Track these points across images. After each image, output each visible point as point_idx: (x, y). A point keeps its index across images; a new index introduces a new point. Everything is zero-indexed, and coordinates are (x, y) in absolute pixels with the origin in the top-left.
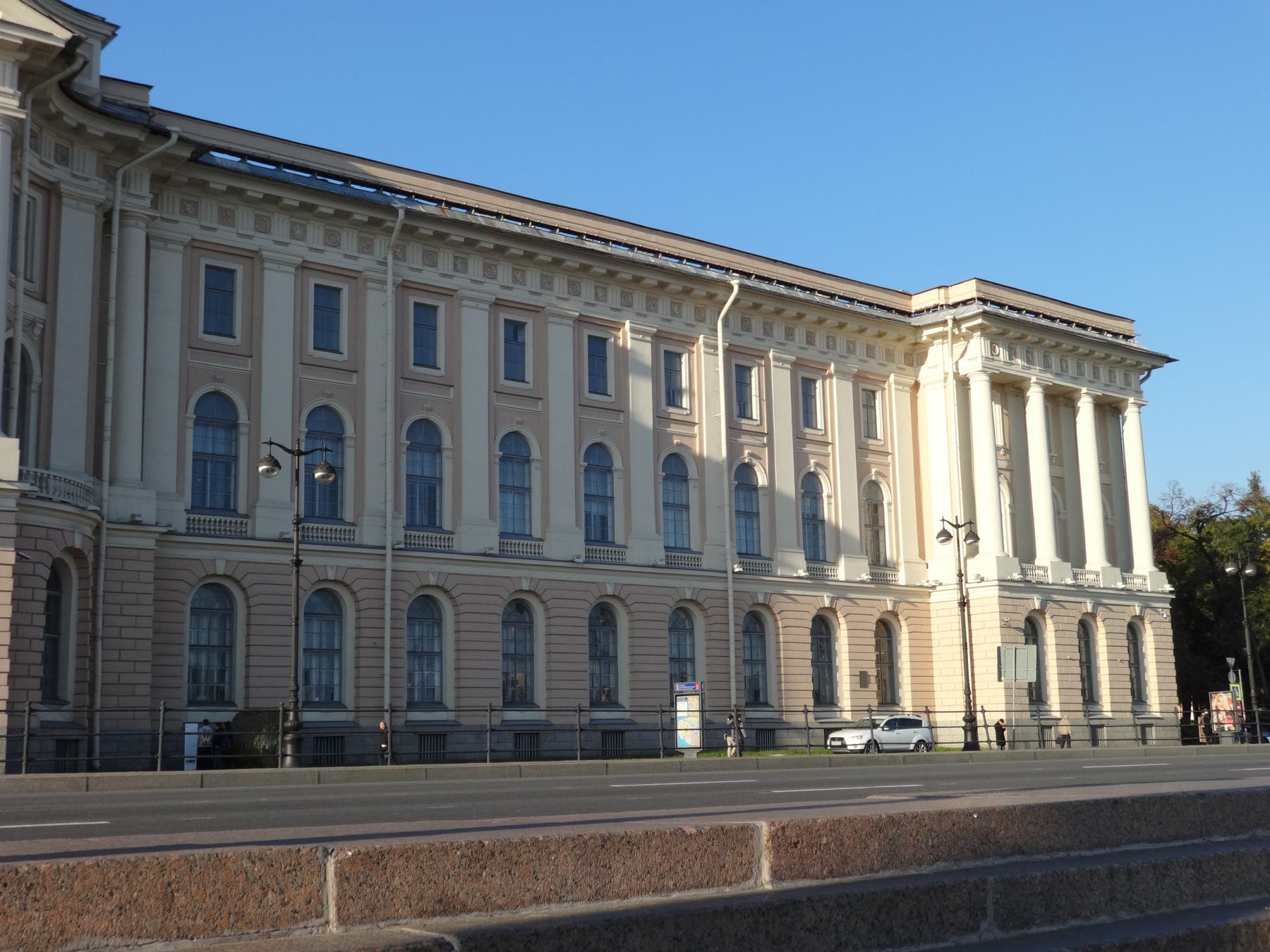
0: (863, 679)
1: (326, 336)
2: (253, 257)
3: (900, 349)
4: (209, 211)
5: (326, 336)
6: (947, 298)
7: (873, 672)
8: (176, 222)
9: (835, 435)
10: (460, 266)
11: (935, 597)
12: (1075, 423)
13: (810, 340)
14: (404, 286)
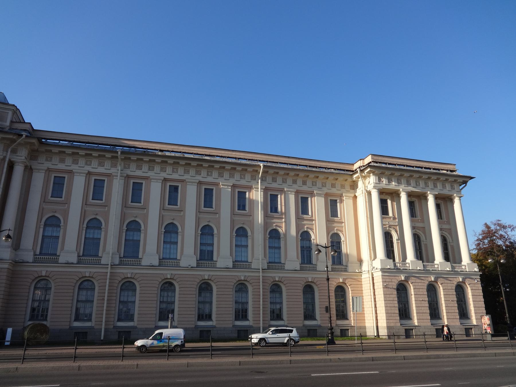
2: (70, 172)
3: (347, 185)
4: (56, 159)
6: (363, 163)
8: (43, 163)
9: (316, 217)
10: (187, 172)
12: (453, 207)
13: (304, 183)
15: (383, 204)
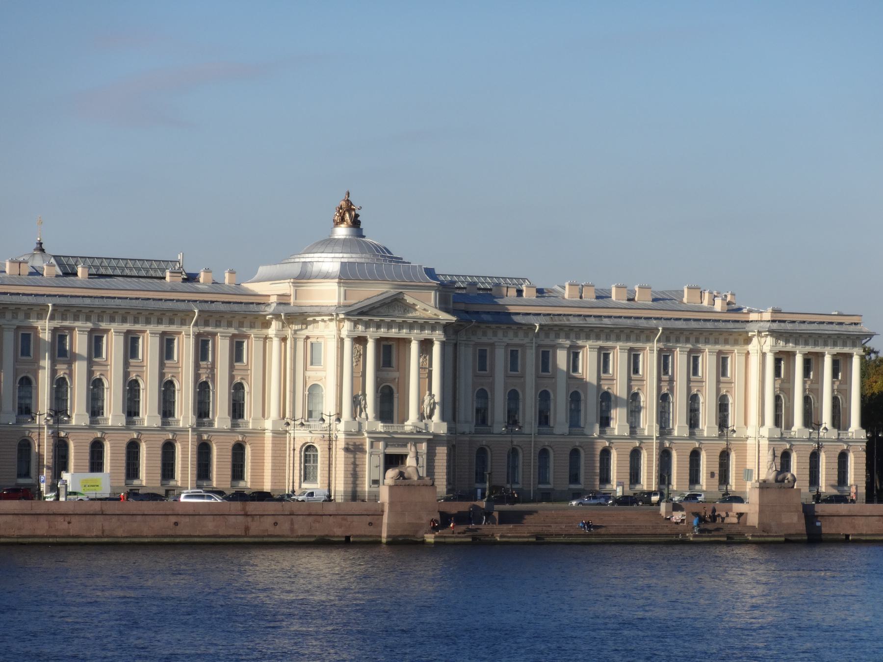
0: (712, 475)
1: (514, 367)
2: (492, 345)
5: (514, 366)
7: (717, 472)
11: (749, 442)
14: (539, 346)
15: (777, 361)
